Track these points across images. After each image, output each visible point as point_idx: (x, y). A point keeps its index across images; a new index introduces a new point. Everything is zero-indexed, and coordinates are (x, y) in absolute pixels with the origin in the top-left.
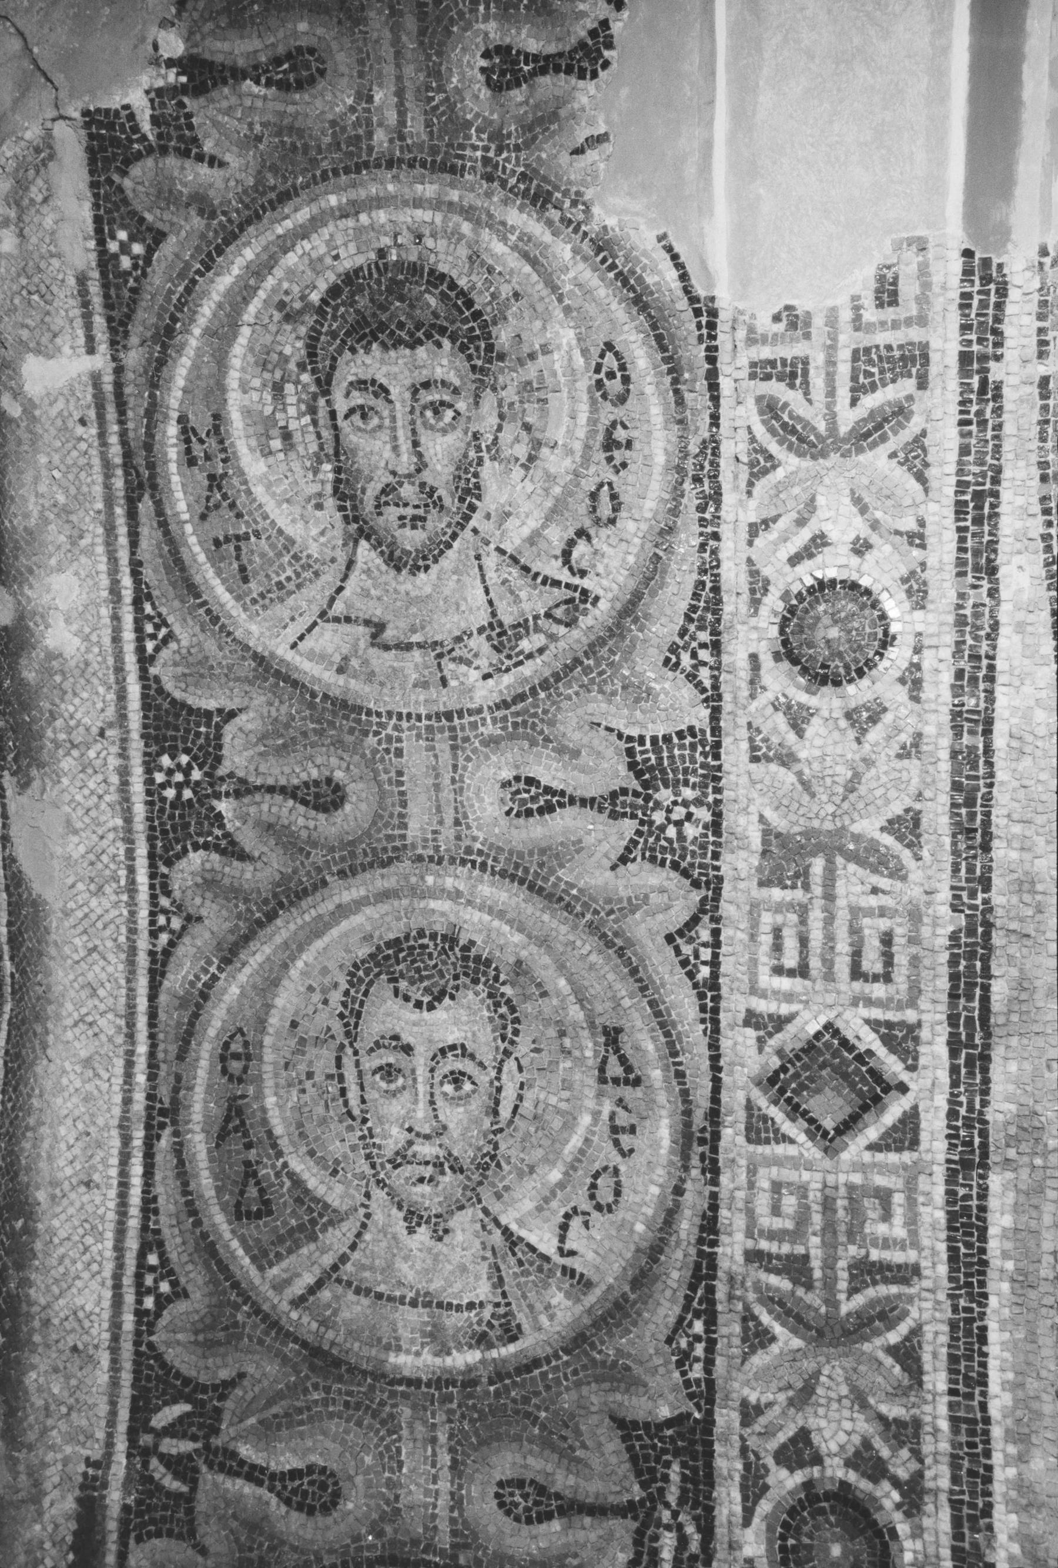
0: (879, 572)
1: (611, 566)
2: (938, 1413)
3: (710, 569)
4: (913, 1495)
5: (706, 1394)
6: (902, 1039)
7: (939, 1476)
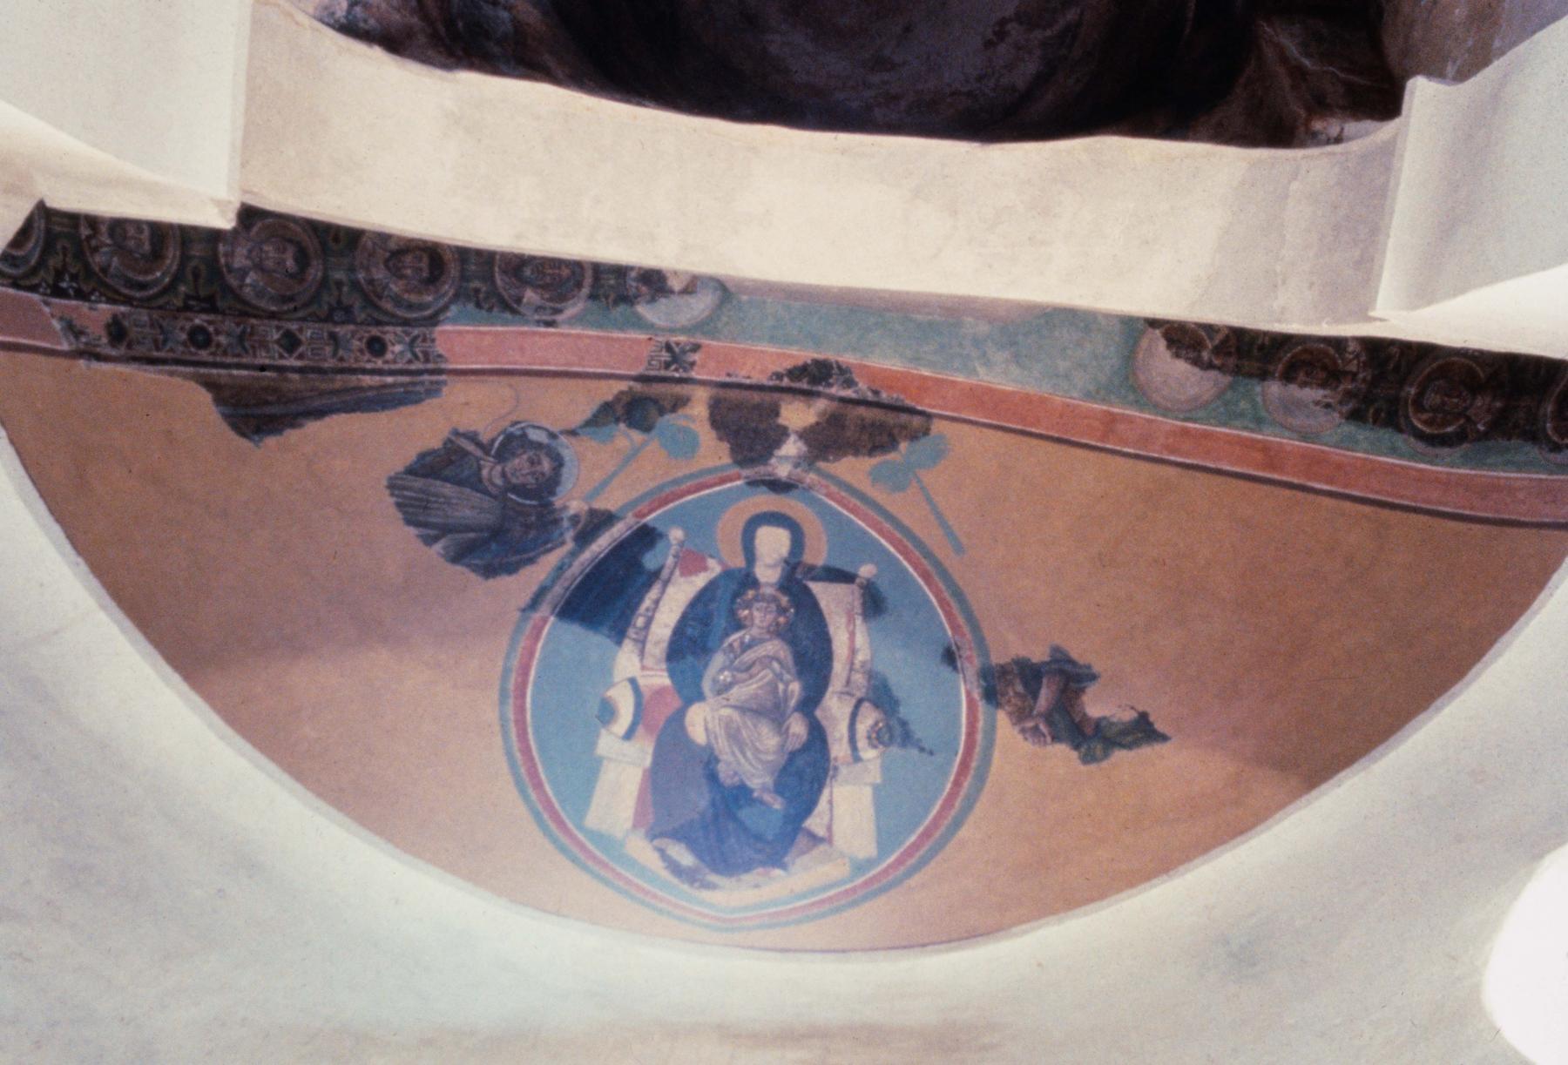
0: (389, 356)
1: (388, 306)
2: (229, 360)
3: (388, 324)
4: (213, 354)
5: (223, 313)
6: (301, 357)
7: (218, 359)
